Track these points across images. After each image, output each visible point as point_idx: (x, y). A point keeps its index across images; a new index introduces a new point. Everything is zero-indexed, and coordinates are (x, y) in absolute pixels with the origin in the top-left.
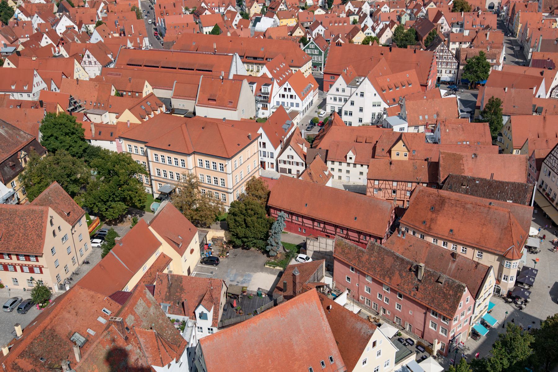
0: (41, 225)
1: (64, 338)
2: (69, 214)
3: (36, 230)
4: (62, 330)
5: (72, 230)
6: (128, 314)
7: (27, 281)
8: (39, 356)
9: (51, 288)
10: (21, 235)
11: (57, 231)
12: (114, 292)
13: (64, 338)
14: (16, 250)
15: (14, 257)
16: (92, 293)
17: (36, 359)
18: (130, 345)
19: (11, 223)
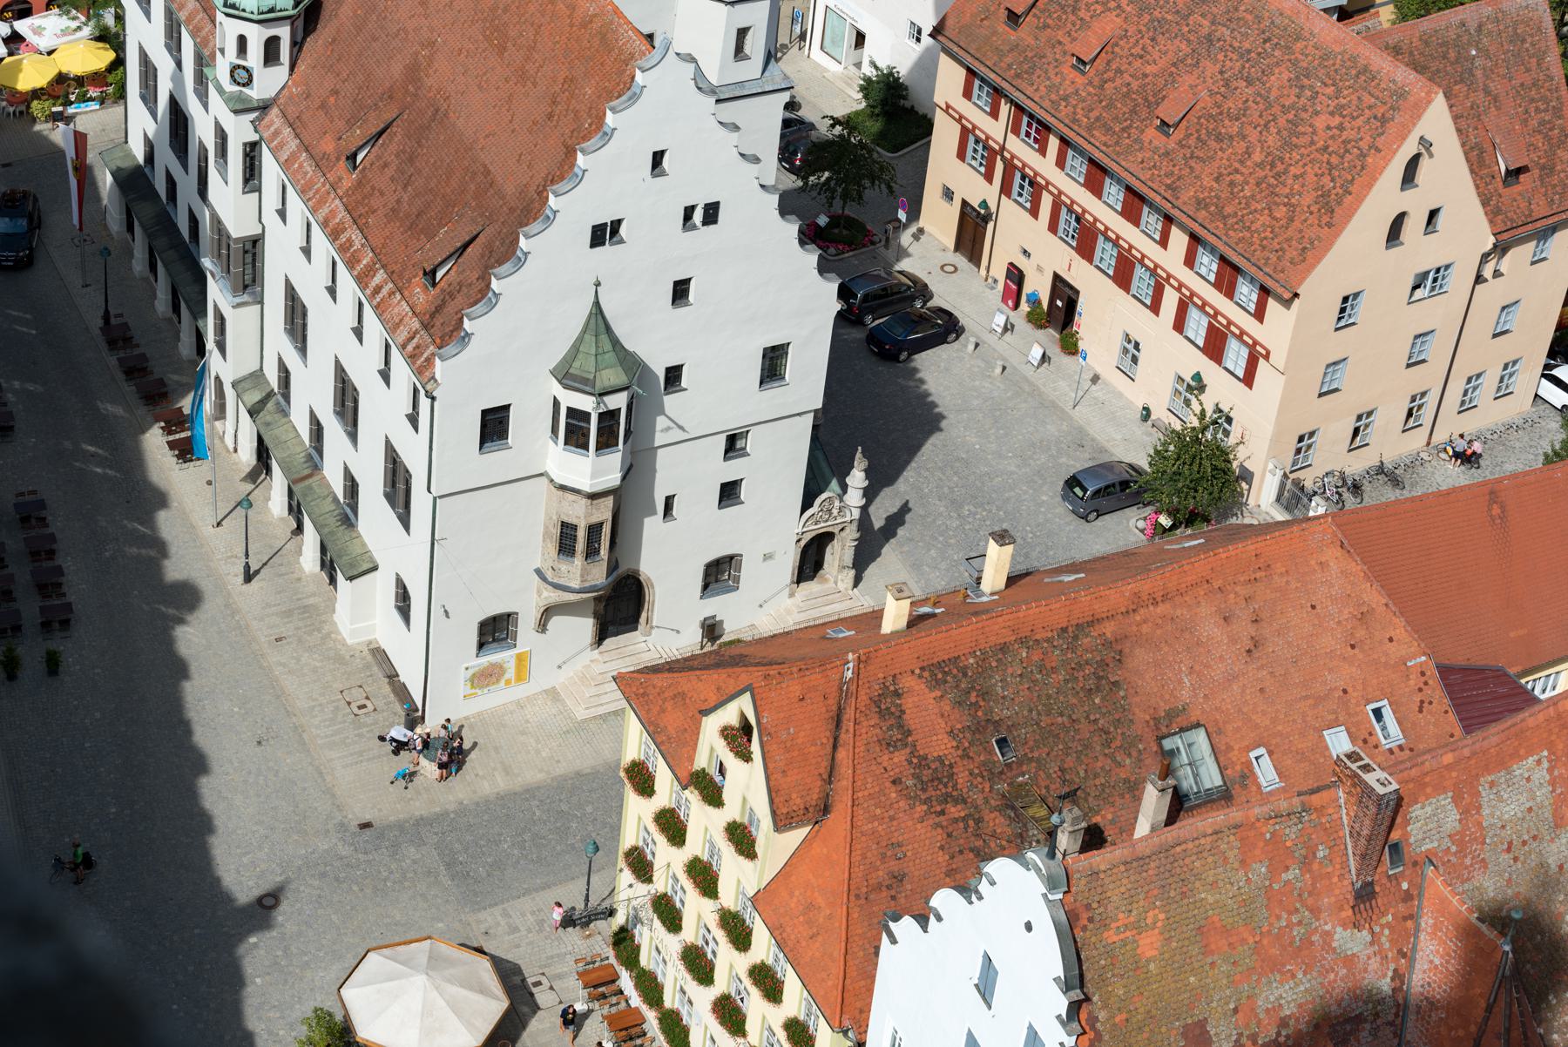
0: (1363, 155)
1: (1141, 716)
2: (1514, 174)
3: (1331, 167)
4: (1155, 679)
5: (1485, 257)
6: (1440, 789)
7: (1169, 384)
8: (997, 724)
9: (1247, 476)
10: (1257, 157)
11: (1413, 229)
12: (1478, 661)
13: (1141, 716)
14: (1202, 215)
15: (1179, 240)
16: (1374, 597)
17: (978, 729)
18: (1365, 934)
19: (1249, 83)
